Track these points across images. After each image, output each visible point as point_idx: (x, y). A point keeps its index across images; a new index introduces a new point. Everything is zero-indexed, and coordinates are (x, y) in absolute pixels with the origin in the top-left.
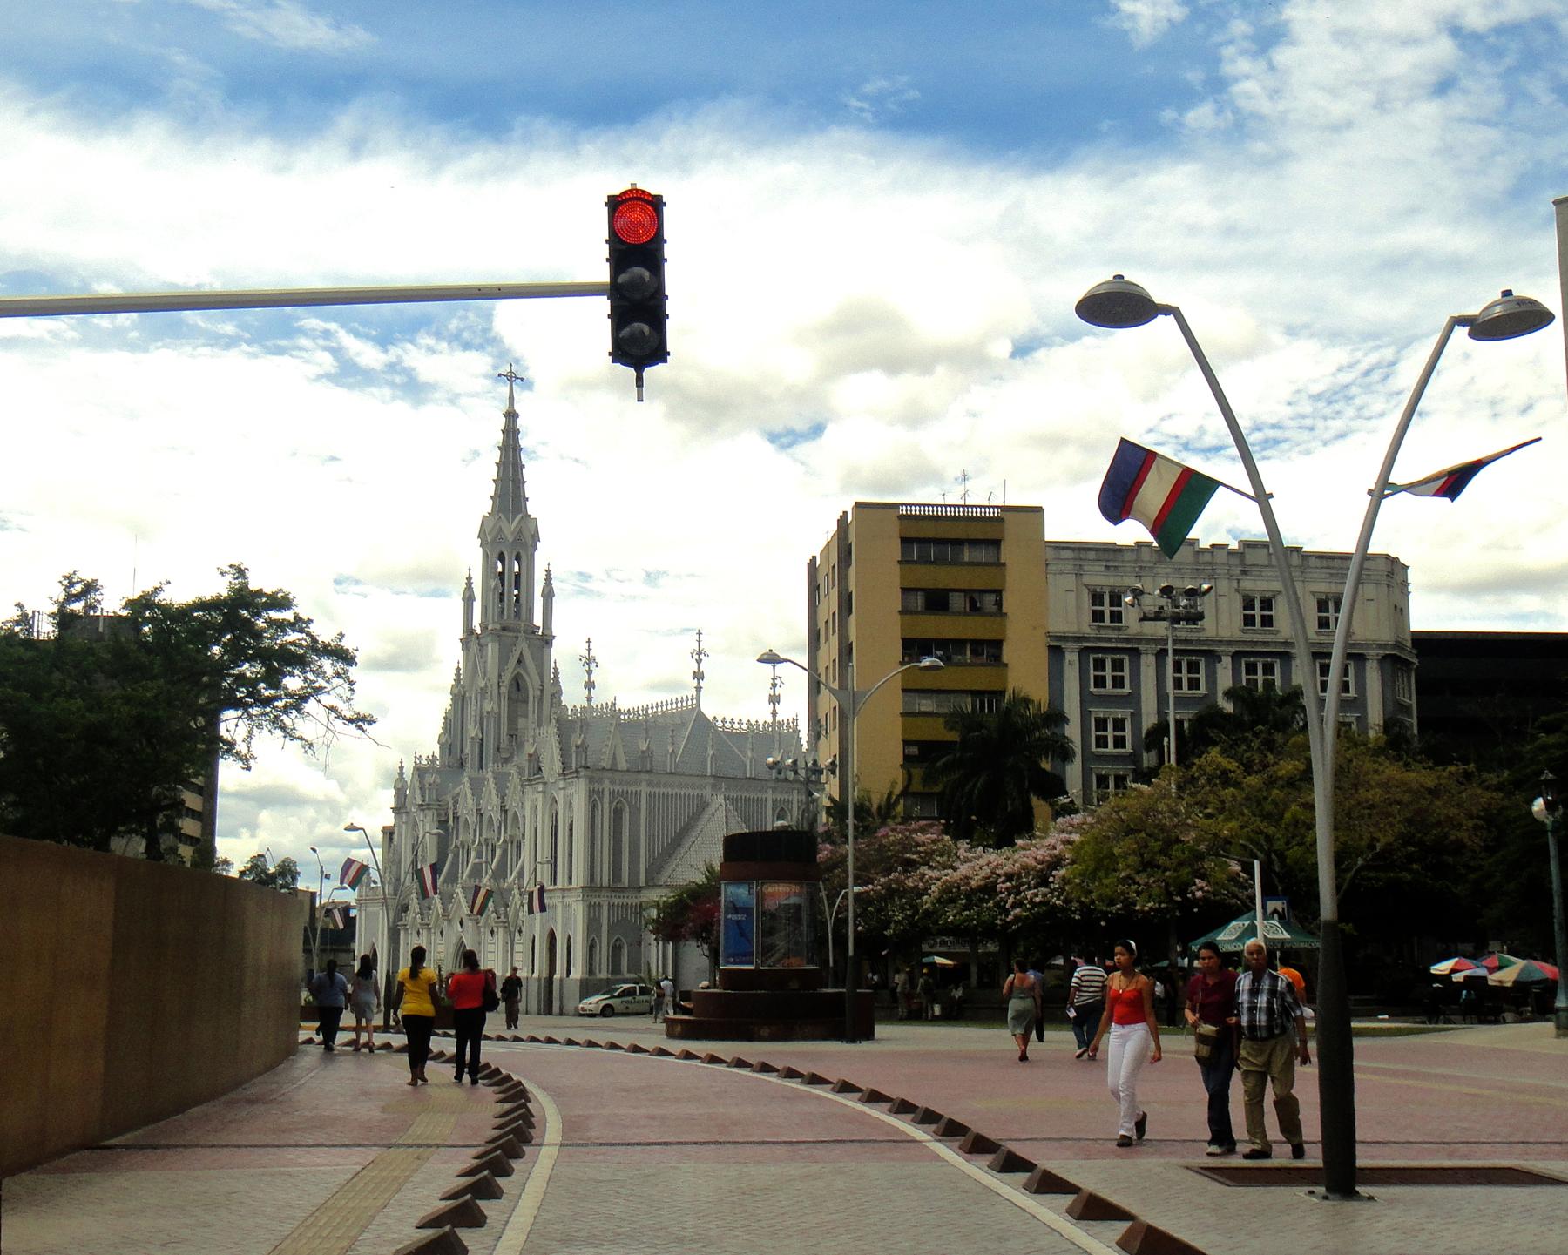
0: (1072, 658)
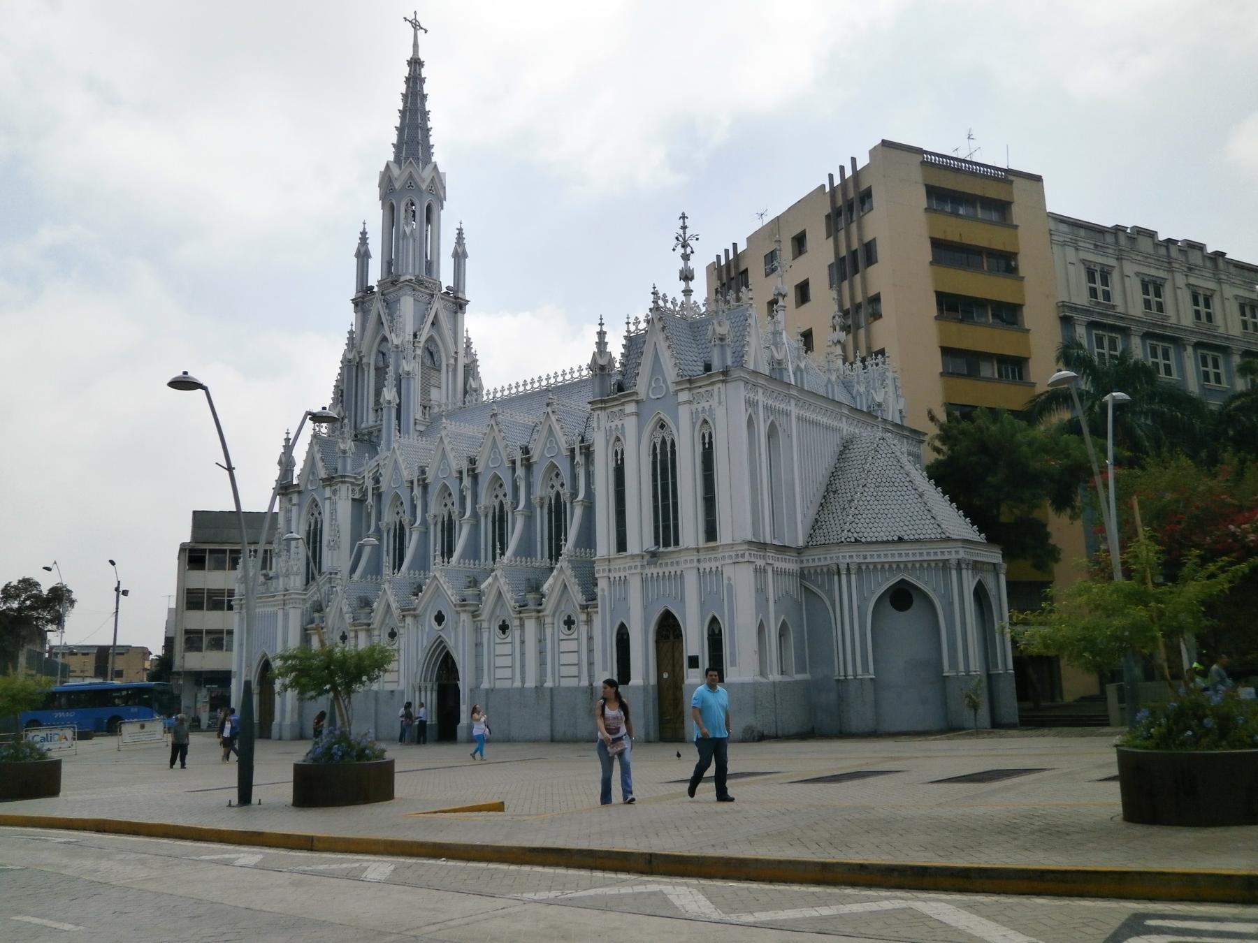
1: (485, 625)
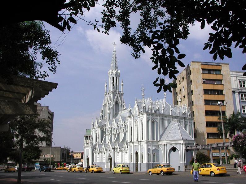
0: (237, 94)
1: (115, 152)
